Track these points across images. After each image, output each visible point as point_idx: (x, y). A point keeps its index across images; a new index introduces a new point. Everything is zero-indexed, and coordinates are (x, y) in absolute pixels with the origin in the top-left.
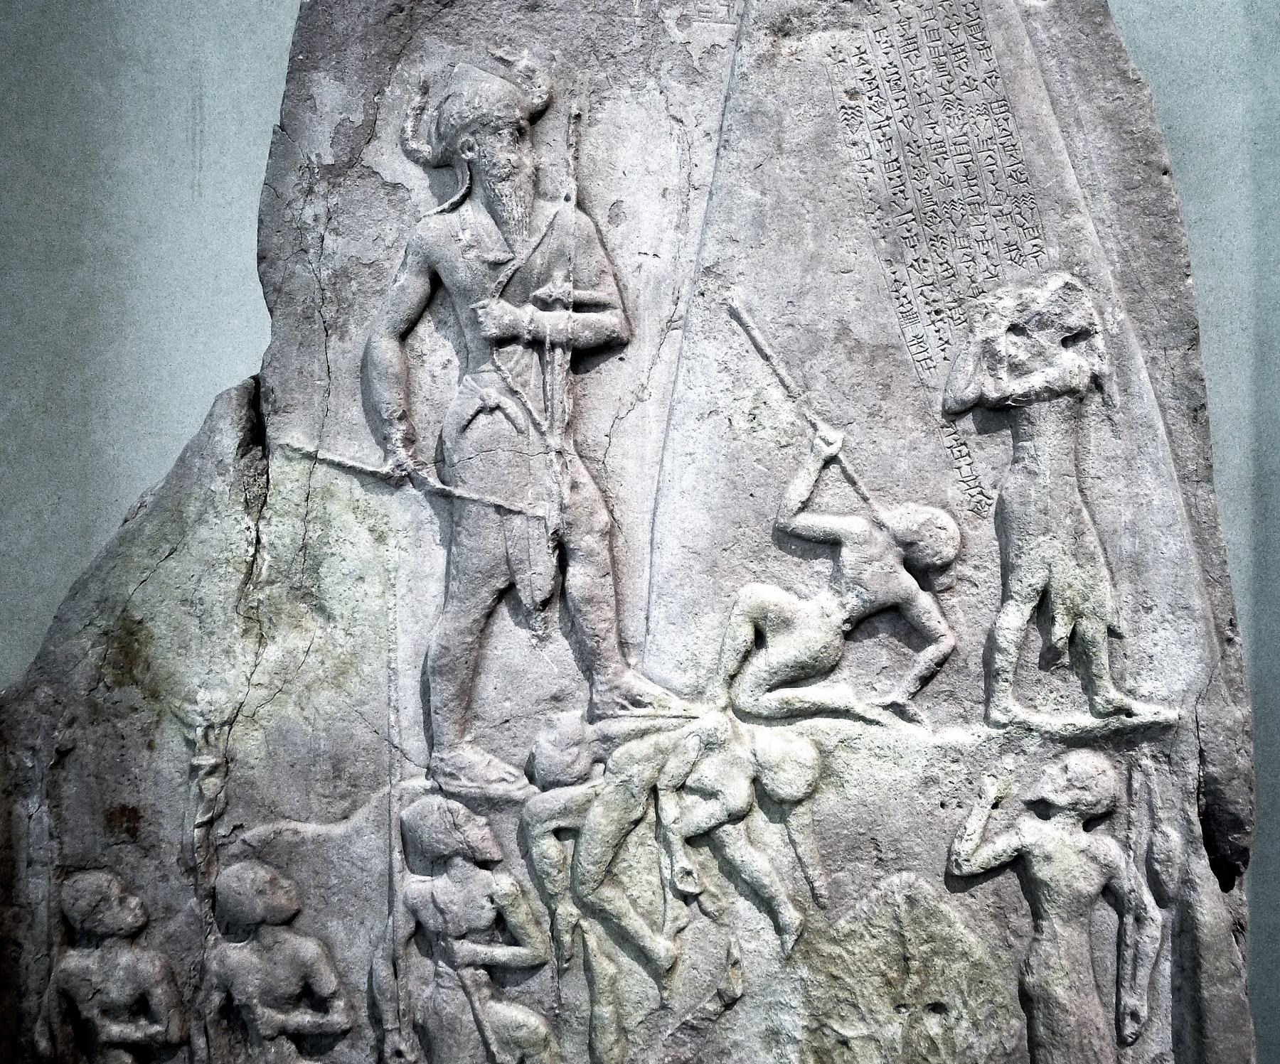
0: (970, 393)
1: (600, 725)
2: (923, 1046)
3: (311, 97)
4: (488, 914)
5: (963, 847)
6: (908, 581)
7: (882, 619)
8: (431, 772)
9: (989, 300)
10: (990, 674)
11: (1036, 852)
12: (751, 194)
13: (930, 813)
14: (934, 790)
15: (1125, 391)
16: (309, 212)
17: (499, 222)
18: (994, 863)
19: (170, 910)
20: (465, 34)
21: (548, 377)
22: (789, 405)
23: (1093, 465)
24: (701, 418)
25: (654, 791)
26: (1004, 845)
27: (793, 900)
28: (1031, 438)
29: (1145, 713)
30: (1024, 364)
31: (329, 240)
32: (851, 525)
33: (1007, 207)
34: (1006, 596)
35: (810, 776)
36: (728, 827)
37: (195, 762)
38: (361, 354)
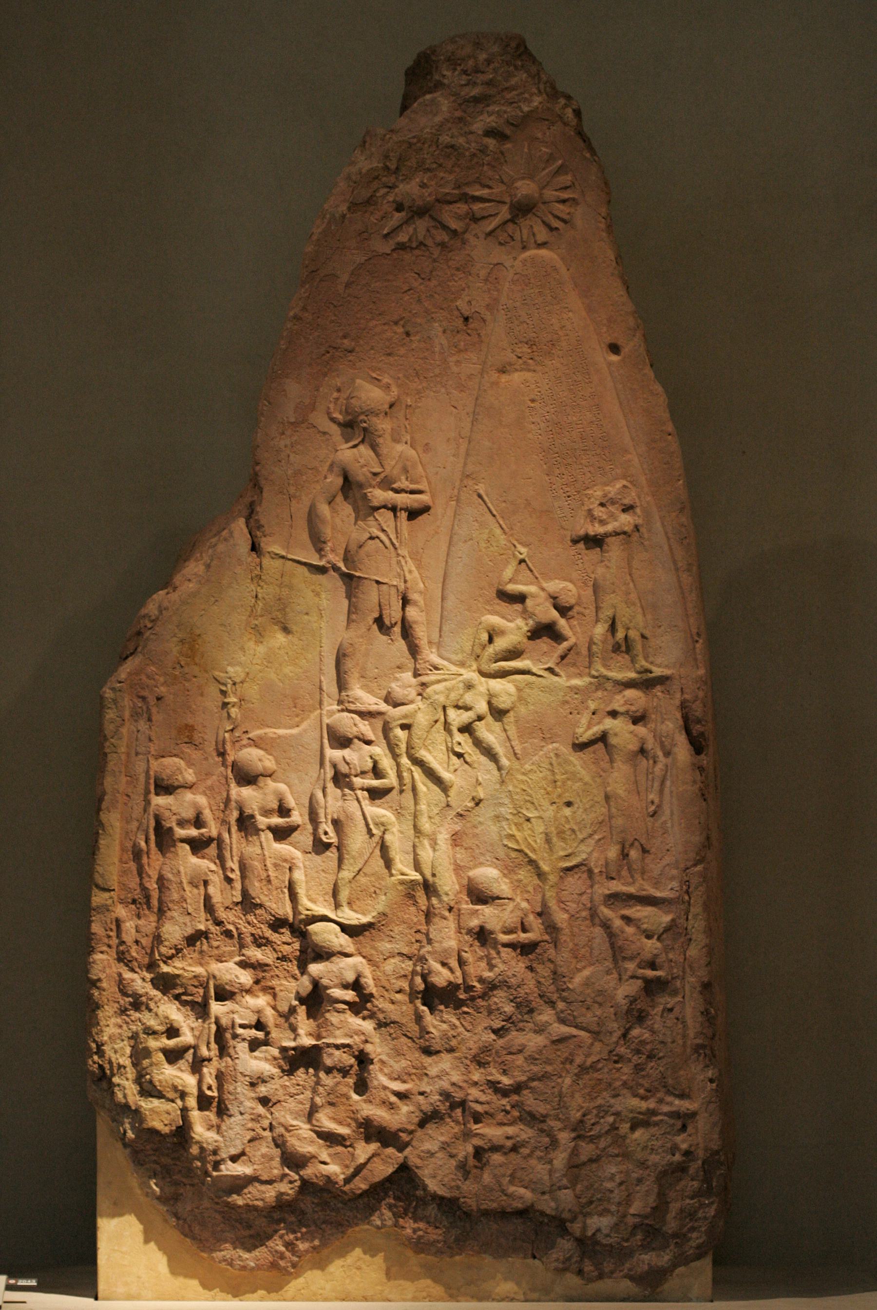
0: (582, 532)
1: (419, 678)
2: (563, 819)
3: (284, 390)
4: (370, 764)
5: (580, 731)
6: (555, 614)
7: (544, 631)
8: (340, 702)
9: (590, 492)
10: (591, 655)
11: (611, 732)
12: (487, 444)
13: (566, 717)
14: (567, 706)
15: (649, 531)
16: (282, 444)
17: (377, 455)
18: (593, 738)
19: (209, 774)
20: (358, 364)
21: (398, 524)
22: (503, 537)
23: (635, 564)
24: (465, 541)
25: (444, 708)
26: (596, 729)
27: (506, 756)
28: (608, 552)
29: (657, 671)
30: (604, 520)
31: (292, 456)
32: (532, 589)
33: (598, 451)
34: (597, 621)
35: (514, 698)
36: (477, 723)
37: (226, 700)
38: (307, 510)
